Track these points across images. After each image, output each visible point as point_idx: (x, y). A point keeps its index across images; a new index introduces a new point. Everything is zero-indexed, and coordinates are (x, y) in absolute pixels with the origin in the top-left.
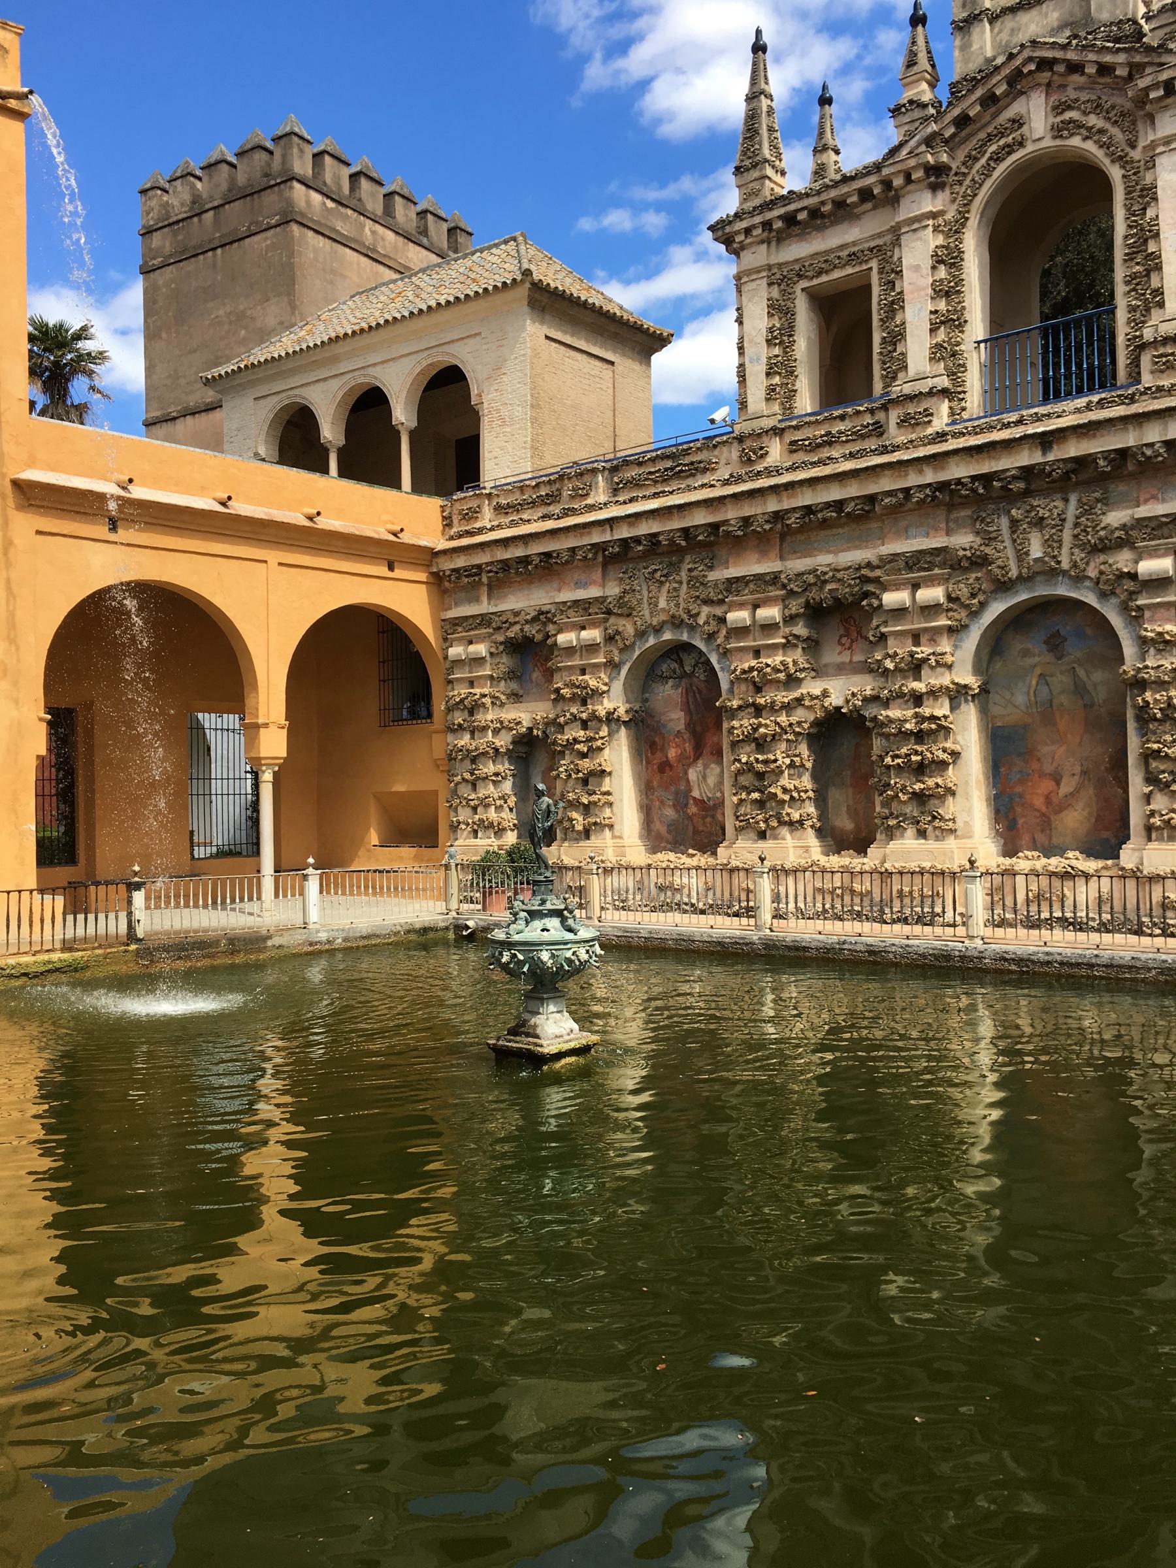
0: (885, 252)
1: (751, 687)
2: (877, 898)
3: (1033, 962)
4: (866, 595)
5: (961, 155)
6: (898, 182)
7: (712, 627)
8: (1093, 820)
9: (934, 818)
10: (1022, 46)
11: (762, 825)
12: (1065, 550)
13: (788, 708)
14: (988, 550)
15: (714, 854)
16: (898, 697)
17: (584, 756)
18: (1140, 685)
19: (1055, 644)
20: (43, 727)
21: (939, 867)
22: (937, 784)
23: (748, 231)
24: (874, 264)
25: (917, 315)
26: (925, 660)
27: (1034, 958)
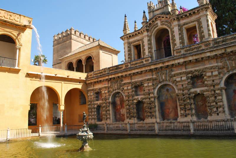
0: (142, 40)
4: (142, 84)
5: (150, 28)
6: (143, 31)
10: (156, 15)
11: (130, 117)
12: (167, 77)
13: (133, 100)
15: (124, 122)
17: (106, 108)
18: (178, 95)
19: (167, 90)
20: (30, 106)
23: (125, 38)
24: (141, 41)
25: (146, 47)
26: (150, 93)
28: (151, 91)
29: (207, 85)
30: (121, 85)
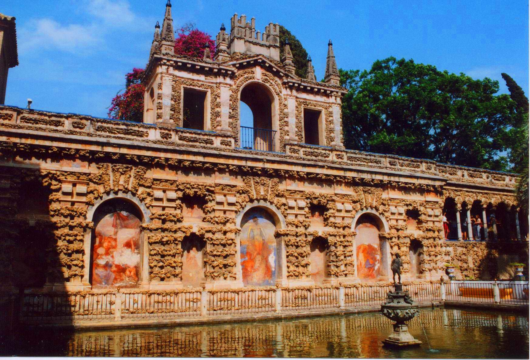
1: (161, 221)
7: (144, 196)
14: (249, 189)
16: (219, 231)
17: (70, 242)
23: (168, 61)
26: (228, 220)
28: (230, 217)
29: (336, 225)
30: (140, 183)
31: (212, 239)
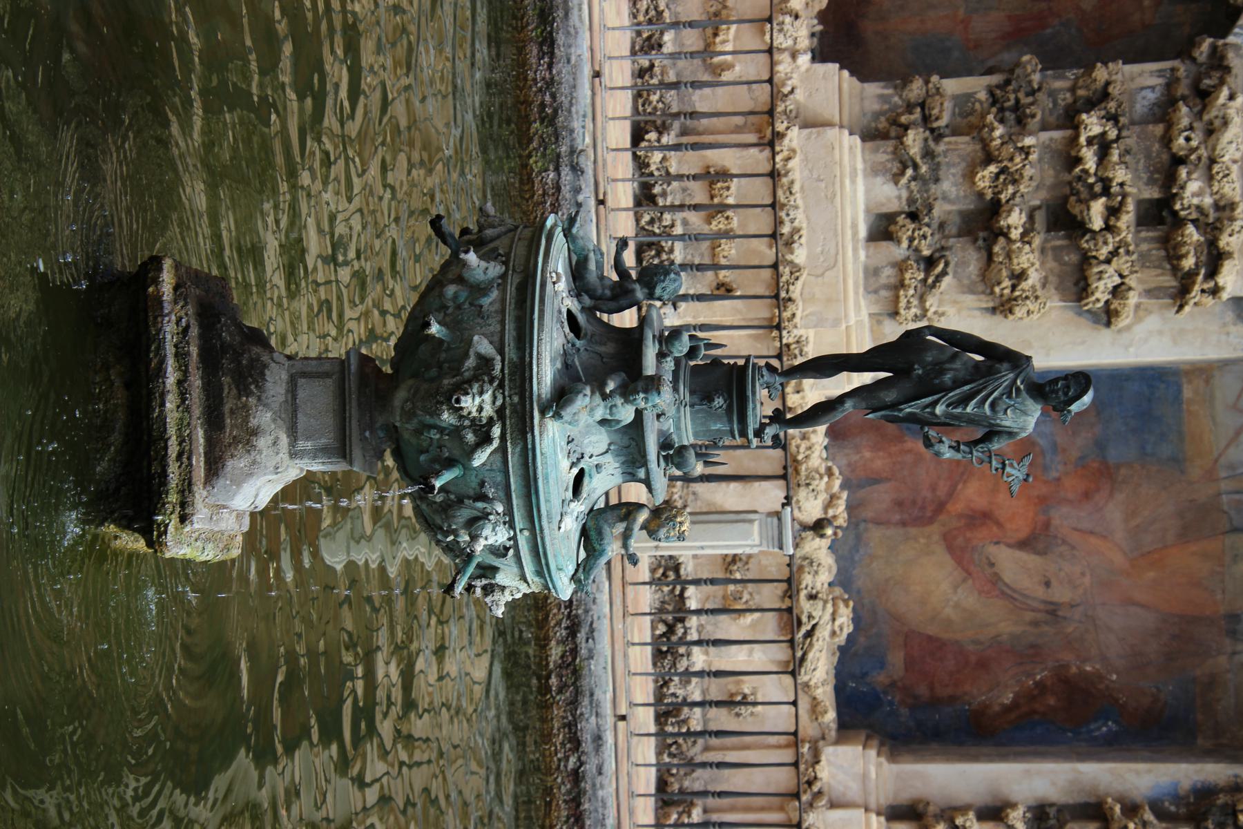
2: (702, 100)
3: (574, 703)
8: (932, 630)
9: (930, 262)
21: (796, 291)
22: (1020, 277)
27: (585, 706)
31: (1204, 96)
